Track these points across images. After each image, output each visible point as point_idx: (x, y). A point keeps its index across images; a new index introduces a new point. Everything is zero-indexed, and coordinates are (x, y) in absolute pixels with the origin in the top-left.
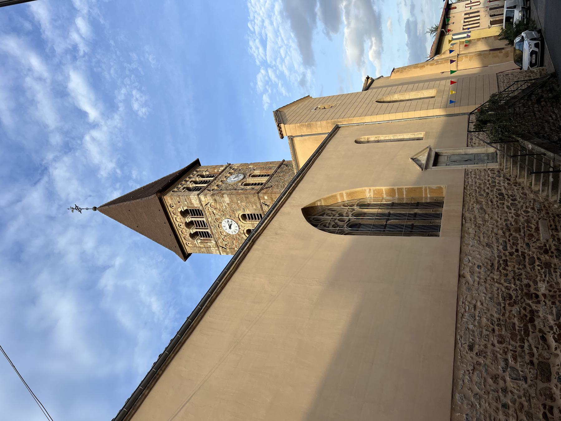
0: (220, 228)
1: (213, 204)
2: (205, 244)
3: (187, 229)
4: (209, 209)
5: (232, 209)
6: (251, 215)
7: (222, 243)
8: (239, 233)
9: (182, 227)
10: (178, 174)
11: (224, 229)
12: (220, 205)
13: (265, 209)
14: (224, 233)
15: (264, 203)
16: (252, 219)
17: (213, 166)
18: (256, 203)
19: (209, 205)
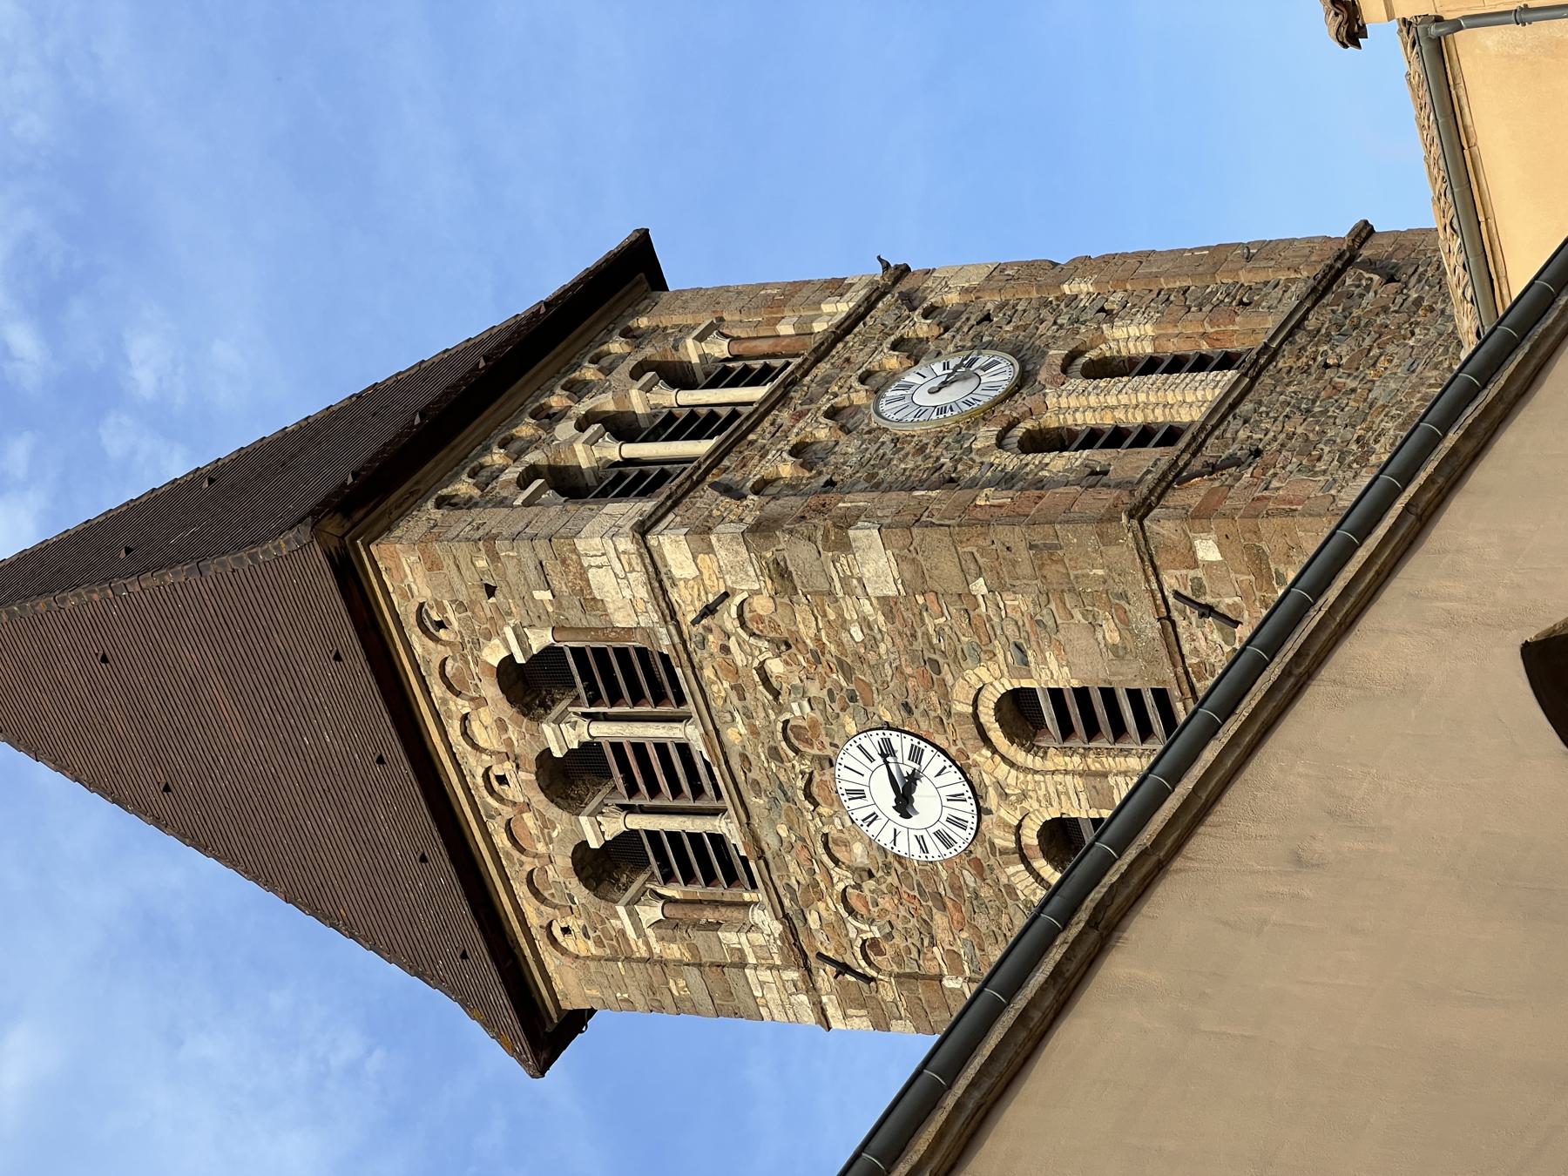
0: (824, 810)
1: (762, 605)
2: (699, 938)
3: (553, 812)
4: (733, 644)
5: (919, 644)
6: (1082, 694)
7: (836, 928)
8: (979, 852)
9: (512, 792)
10: (486, 359)
11: (859, 815)
12: (825, 615)
13: (1196, 651)
14: (858, 848)
15: (1188, 593)
16: (1092, 731)
17: (764, 286)
18: (1123, 596)
19: (728, 617)
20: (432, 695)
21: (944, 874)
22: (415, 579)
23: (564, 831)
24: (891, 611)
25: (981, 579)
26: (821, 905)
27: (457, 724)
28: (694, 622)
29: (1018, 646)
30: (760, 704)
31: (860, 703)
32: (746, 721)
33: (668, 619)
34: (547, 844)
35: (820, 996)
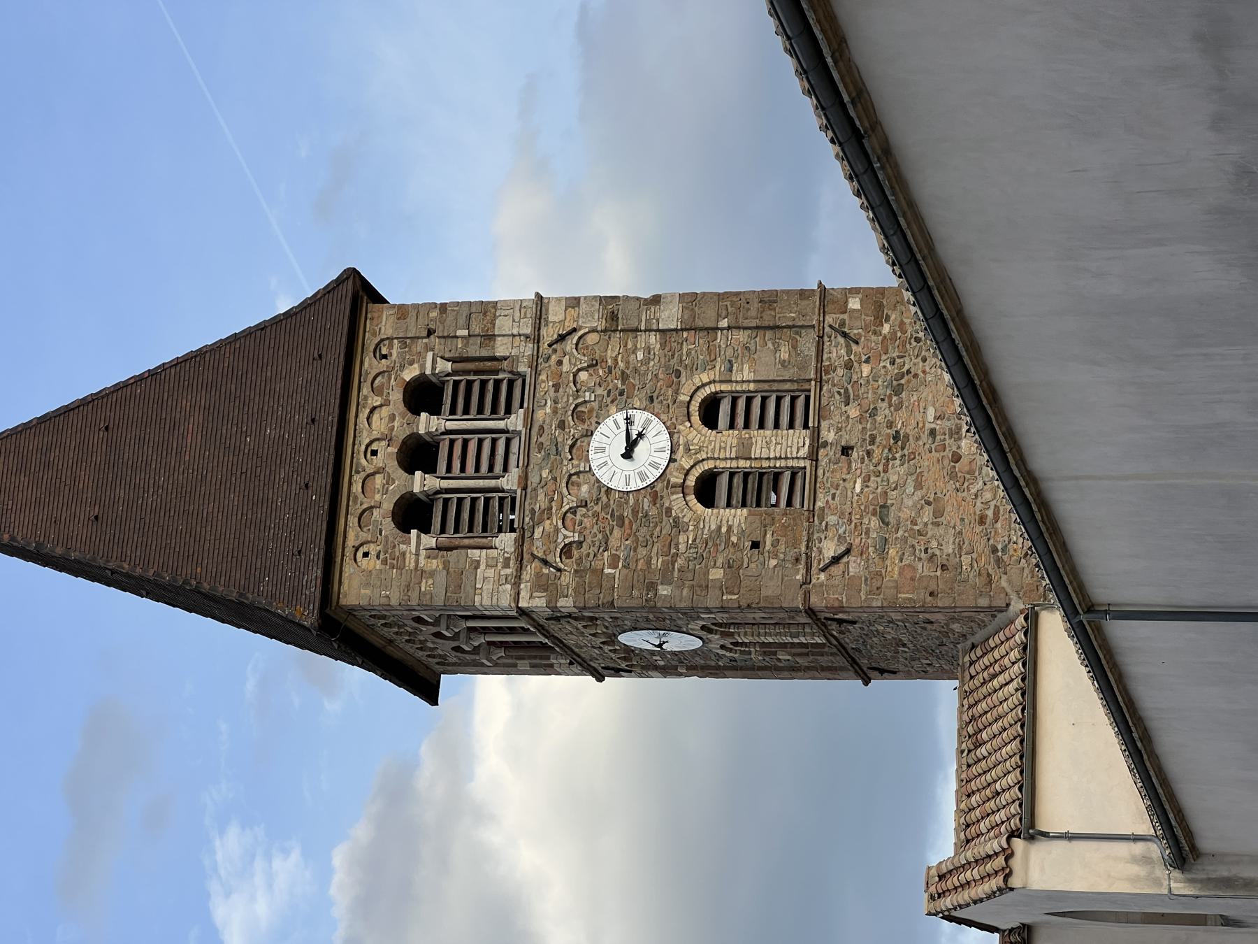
4: (566, 360)
5: (672, 362)
7: (550, 537)
12: (626, 346)
15: (837, 326)
19: (570, 344)
20: (361, 393)
21: (631, 502)
22: (386, 323)
23: (398, 486)
24: (665, 343)
25: (726, 319)
26: (548, 522)
27: (367, 411)
28: (550, 345)
29: (730, 362)
30: (566, 394)
31: (625, 397)
32: (553, 405)
33: (536, 341)
34: (383, 495)
35: (520, 584)
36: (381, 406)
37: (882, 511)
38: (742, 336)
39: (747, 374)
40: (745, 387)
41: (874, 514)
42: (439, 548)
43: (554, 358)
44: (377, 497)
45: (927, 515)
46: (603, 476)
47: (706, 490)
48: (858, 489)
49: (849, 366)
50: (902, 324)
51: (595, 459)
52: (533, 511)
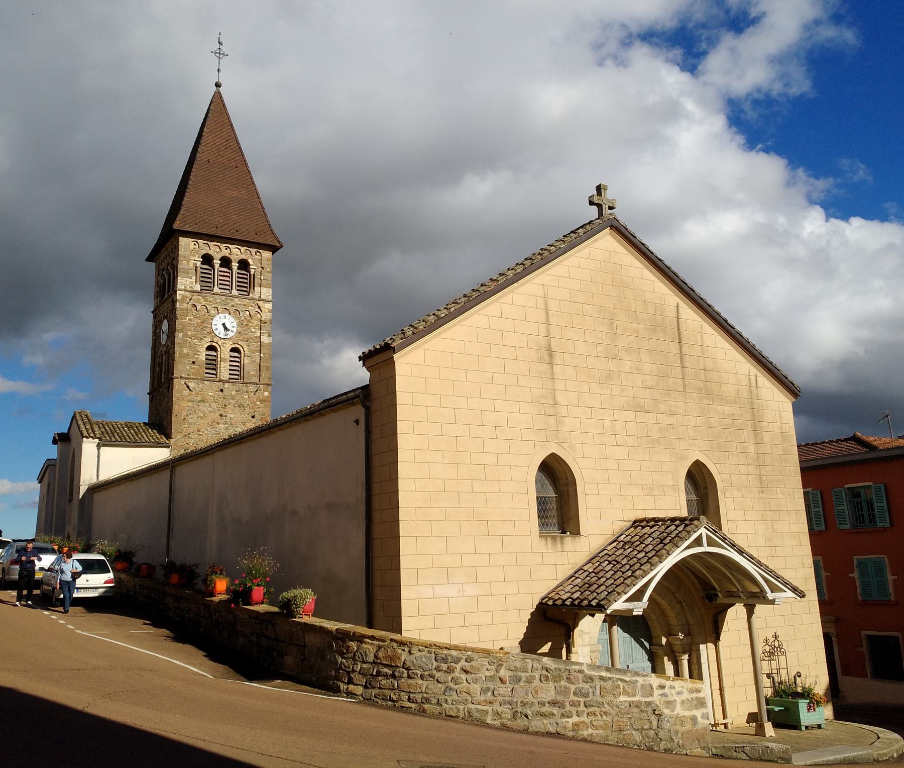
4: (253, 308)
13: (250, 386)
21: (209, 326)
26: (203, 300)
36: (241, 252)
37: (203, 401)
38: (258, 360)
39: (246, 361)
40: (242, 361)
41: (202, 398)
42: (196, 267)
43: (253, 305)
44: (213, 249)
45: (201, 414)
46: (217, 318)
47: (211, 348)
48: (210, 394)
49: (247, 392)
50: (260, 408)
51: (222, 315)
52: (207, 296)
